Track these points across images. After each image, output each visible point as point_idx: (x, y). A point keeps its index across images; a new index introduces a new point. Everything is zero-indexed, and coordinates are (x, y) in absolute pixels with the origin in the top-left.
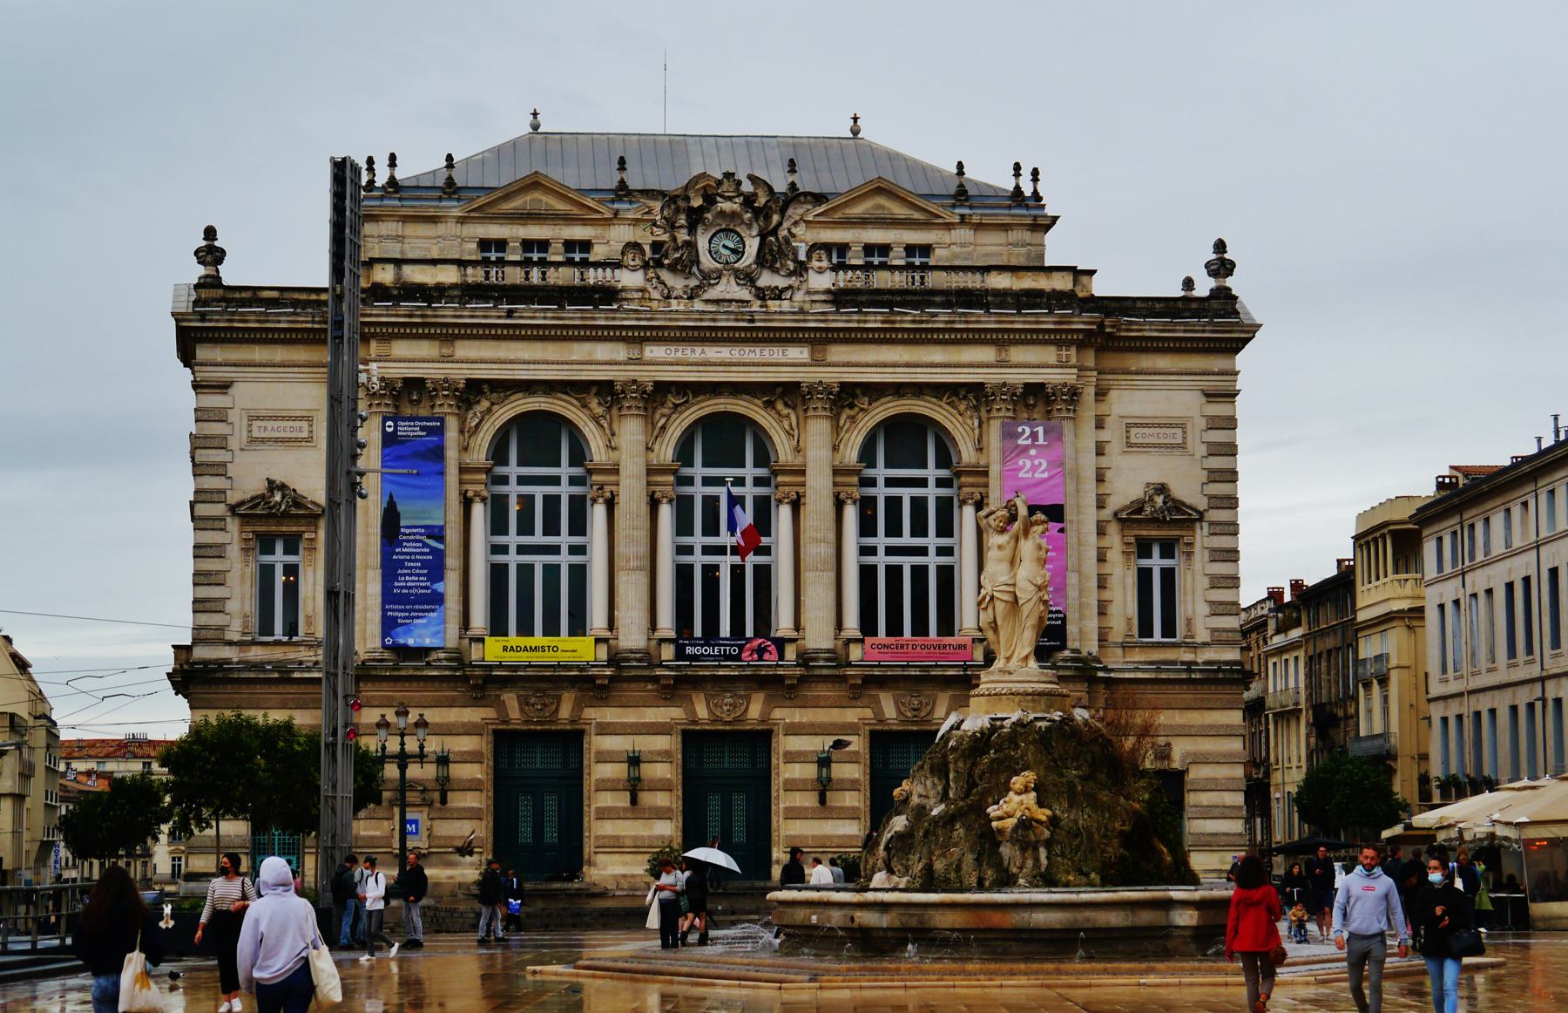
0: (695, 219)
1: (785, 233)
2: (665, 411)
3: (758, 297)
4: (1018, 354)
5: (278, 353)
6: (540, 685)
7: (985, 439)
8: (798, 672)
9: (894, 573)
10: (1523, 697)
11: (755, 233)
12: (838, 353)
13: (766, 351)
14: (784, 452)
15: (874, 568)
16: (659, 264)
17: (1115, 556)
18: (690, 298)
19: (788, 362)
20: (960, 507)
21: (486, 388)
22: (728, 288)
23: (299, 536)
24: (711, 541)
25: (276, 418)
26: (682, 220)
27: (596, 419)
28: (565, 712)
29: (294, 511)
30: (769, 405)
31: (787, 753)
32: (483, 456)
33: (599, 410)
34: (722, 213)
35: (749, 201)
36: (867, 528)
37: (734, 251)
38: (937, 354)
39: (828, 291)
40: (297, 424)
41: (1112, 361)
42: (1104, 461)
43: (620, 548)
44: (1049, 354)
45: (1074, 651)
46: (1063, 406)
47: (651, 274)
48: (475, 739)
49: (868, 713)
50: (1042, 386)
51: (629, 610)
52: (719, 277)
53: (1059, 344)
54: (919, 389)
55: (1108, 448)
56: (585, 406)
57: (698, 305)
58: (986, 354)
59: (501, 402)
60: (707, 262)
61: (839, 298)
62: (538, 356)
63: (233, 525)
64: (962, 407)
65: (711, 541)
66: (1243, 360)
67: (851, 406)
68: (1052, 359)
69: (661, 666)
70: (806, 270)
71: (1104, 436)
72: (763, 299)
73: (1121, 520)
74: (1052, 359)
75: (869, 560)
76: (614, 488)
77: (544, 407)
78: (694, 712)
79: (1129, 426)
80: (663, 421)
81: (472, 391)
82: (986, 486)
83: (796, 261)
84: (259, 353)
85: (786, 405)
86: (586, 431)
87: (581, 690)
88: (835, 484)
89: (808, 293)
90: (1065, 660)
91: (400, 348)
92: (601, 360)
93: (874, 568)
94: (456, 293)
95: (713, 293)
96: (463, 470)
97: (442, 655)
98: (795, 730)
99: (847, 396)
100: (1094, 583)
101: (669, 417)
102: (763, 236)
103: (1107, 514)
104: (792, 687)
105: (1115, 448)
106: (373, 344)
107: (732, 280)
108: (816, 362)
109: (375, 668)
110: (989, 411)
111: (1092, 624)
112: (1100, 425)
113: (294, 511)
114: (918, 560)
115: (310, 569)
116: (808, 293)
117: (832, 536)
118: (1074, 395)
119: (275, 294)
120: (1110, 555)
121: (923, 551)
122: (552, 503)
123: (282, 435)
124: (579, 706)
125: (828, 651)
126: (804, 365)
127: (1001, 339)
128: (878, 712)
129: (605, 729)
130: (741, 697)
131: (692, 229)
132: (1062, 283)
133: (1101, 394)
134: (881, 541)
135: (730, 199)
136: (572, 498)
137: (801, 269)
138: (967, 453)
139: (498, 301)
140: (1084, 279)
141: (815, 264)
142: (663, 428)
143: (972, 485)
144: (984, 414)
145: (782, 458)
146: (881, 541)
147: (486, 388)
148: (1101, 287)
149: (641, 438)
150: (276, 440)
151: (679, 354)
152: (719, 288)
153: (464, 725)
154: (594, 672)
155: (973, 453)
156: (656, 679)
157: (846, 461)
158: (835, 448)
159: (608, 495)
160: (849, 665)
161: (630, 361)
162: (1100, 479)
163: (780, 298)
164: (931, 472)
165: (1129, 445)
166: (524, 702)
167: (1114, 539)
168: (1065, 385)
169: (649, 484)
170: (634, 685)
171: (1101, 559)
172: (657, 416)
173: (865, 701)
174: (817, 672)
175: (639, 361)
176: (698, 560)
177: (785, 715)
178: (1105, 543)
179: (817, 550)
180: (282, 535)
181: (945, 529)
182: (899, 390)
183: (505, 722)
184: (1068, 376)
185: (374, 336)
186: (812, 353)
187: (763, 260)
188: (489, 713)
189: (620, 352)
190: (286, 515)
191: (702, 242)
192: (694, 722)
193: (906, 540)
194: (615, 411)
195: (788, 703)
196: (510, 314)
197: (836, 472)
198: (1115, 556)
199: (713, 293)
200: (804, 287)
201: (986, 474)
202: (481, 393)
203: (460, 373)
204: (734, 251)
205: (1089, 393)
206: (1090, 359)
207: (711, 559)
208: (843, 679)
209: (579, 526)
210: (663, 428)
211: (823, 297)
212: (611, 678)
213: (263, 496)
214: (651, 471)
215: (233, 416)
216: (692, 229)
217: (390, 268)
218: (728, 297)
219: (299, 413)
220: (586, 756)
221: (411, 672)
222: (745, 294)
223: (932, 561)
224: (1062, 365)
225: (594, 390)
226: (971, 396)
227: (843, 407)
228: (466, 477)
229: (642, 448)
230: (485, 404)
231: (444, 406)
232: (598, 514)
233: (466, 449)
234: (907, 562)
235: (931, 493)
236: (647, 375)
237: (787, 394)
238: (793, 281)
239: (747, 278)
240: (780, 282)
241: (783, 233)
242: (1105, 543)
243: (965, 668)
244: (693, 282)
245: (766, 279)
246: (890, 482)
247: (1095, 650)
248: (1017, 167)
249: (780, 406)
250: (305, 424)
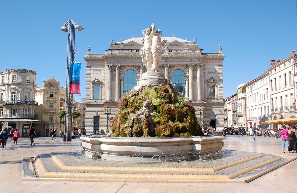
4: (193, 60)
10: (260, 106)
12: (169, 60)
17: (206, 87)
27: (137, 70)
38: (182, 60)
41: (205, 61)
42: (205, 75)
54: (180, 66)
58: (189, 60)
59: (125, 68)
63: (91, 84)
64: (185, 67)
66: (223, 61)
71: (205, 71)
84: (94, 62)
100: (204, 91)
103: (205, 82)
105: (206, 73)
112: (204, 69)
133: (204, 65)
148: (203, 52)
162: (204, 77)
165: (208, 72)
167: (206, 85)
171: (205, 87)
178: (205, 85)
198: (206, 87)
213: (95, 81)
215: (91, 70)
230: (123, 68)
249: (161, 67)
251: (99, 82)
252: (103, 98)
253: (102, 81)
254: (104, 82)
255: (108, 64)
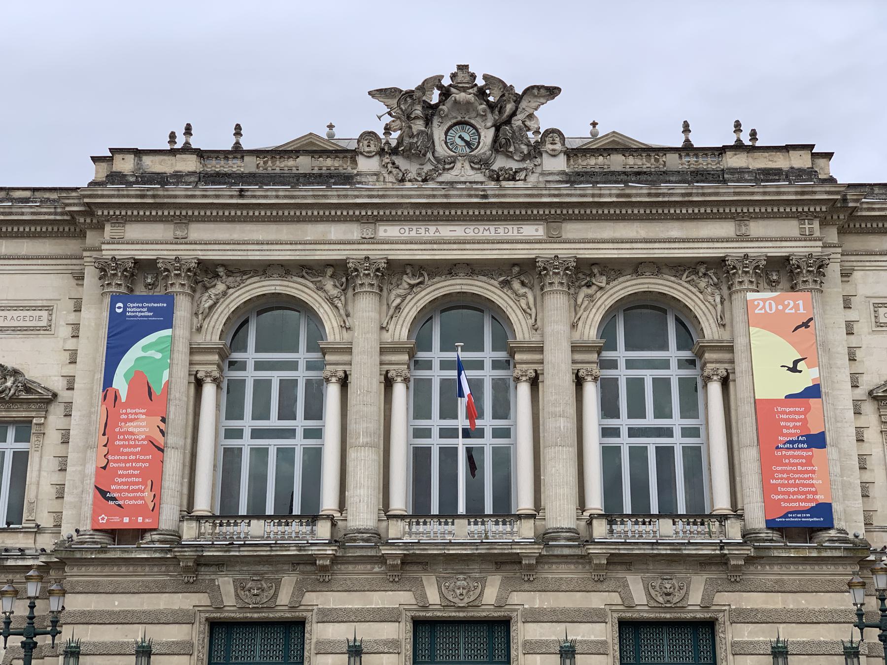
0: (431, 112)
1: (520, 123)
2: (400, 291)
3: (491, 178)
4: (756, 228)
5: (25, 247)
6: (259, 568)
7: (727, 315)
8: (537, 550)
9: (638, 454)
11: (489, 124)
12: (572, 230)
13: (501, 230)
14: (522, 331)
15: (617, 449)
16: (394, 151)
18: (425, 180)
19: (524, 240)
20: (705, 386)
21: (221, 271)
22: (463, 172)
23: (28, 422)
24: (449, 423)
25: (16, 308)
26: (418, 111)
27: (331, 301)
28: (284, 598)
29: (24, 396)
30: (506, 284)
31: (526, 643)
32: (216, 338)
33: (334, 292)
34: (456, 102)
35: (481, 93)
36: (609, 408)
37: (468, 144)
38: (675, 230)
39: (563, 173)
40: (37, 313)
41: (855, 243)
42: (853, 341)
43: (351, 426)
44: (791, 228)
45: (840, 531)
46: (810, 278)
47: (386, 159)
48: (186, 628)
49: (615, 598)
50: (787, 259)
51: (363, 490)
52: (454, 162)
53: (799, 216)
54: (657, 266)
55: (856, 327)
56: (320, 288)
57: (431, 185)
58: (726, 229)
60: (442, 150)
61: (572, 178)
62: (272, 237)
64: (702, 284)
65: (449, 423)
67: (588, 286)
68: (796, 233)
69: (387, 544)
70: (540, 154)
71: (852, 315)
72: (498, 180)
73: (875, 398)
74: (796, 233)
75: (612, 441)
76: (347, 368)
77: (279, 290)
78: (424, 596)
79: (877, 306)
80: (398, 301)
81: (206, 273)
82: (732, 362)
83: (528, 144)
85: (523, 284)
86: (321, 313)
87: (303, 573)
88: (574, 362)
89: (543, 174)
90: (831, 540)
91: (134, 231)
92: (335, 240)
93: (617, 449)
94: (192, 179)
95: (447, 177)
96: (193, 351)
97: (156, 537)
98: (535, 617)
99: (584, 273)
101: (404, 298)
102: (497, 128)
103: (861, 393)
104: (530, 567)
105: (863, 327)
106: (108, 228)
107: (467, 165)
108: (552, 239)
109: (81, 550)
110: (729, 288)
111: (857, 505)
112: (847, 306)
113: (24, 396)
114: (664, 441)
115: (37, 454)
116: (543, 174)
117: (572, 411)
118: (820, 267)
119: (28, 194)
120: (867, 435)
121: (667, 432)
122: (288, 387)
123: (22, 324)
124: (300, 590)
125: (569, 530)
126: (540, 242)
127: (740, 212)
128: (626, 597)
129: (328, 617)
130: (476, 580)
131: (428, 121)
132: (801, 161)
133: (846, 274)
134: (624, 422)
135: (464, 89)
136: (309, 383)
137: (536, 151)
138: (710, 331)
139: (235, 184)
140: (821, 162)
141: (549, 147)
142: (398, 307)
143: (717, 362)
144: (725, 292)
145: (519, 337)
146: (624, 422)
147: (221, 271)
149: (374, 315)
150: (15, 329)
151: (413, 234)
152: (454, 172)
153: (174, 612)
154: (313, 551)
155: (715, 329)
156: (382, 560)
157: (586, 338)
158: (574, 326)
159: (342, 374)
160: (591, 541)
161: (363, 241)
163: (514, 179)
164: (673, 353)
165: (879, 324)
166: (240, 586)
168: (810, 255)
169: (381, 364)
170: (360, 568)
171: (860, 440)
172: (392, 297)
173: (612, 584)
174: (558, 552)
175: (372, 241)
176: (435, 442)
177: (523, 600)
178: (862, 422)
179: (558, 424)
180: (14, 422)
181: (690, 407)
182: (637, 267)
183: (219, 609)
184: (815, 248)
185: (108, 219)
186: (548, 230)
187: (498, 146)
188: (202, 599)
189: (353, 231)
190: (14, 401)
191: (438, 133)
192: (425, 608)
193: (650, 420)
194: (350, 292)
195: (526, 586)
196: (241, 194)
197: (575, 348)
199: (447, 177)
200: (539, 170)
201: (730, 349)
202: (217, 276)
203: (190, 253)
204: (468, 144)
205: (834, 270)
206: (832, 235)
207: (448, 442)
208: (586, 559)
209: (315, 411)
210: (398, 307)
211: (557, 178)
212: (335, 560)
214: (383, 351)
216: (428, 121)
217: (130, 158)
218: (463, 179)
219: (39, 303)
220: (307, 647)
221: (118, 555)
222: (479, 177)
223: (678, 442)
224: (804, 237)
225: (330, 271)
226: (710, 273)
227: (580, 287)
228: (197, 358)
229: (375, 327)
230: (221, 287)
231: (178, 287)
232: (333, 392)
233: (199, 329)
234: (651, 444)
235: (674, 374)
236: (378, 253)
237: (525, 272)
238: (528, 164)
239: (482, 164)
240: (515, 165)
241: (517, 122)
242: (862, 422)
243: (722, 545)
244: (428, 167)
245: (501, 162)
246: (631, 364)
247: (861, 532)
248: (738, 126)
249: (516, 285)
250: (44, 314)
251: (28, 390)
252: (46, 521)
253: (57, 384)
254: (64, 395)
255: (108, 251)
